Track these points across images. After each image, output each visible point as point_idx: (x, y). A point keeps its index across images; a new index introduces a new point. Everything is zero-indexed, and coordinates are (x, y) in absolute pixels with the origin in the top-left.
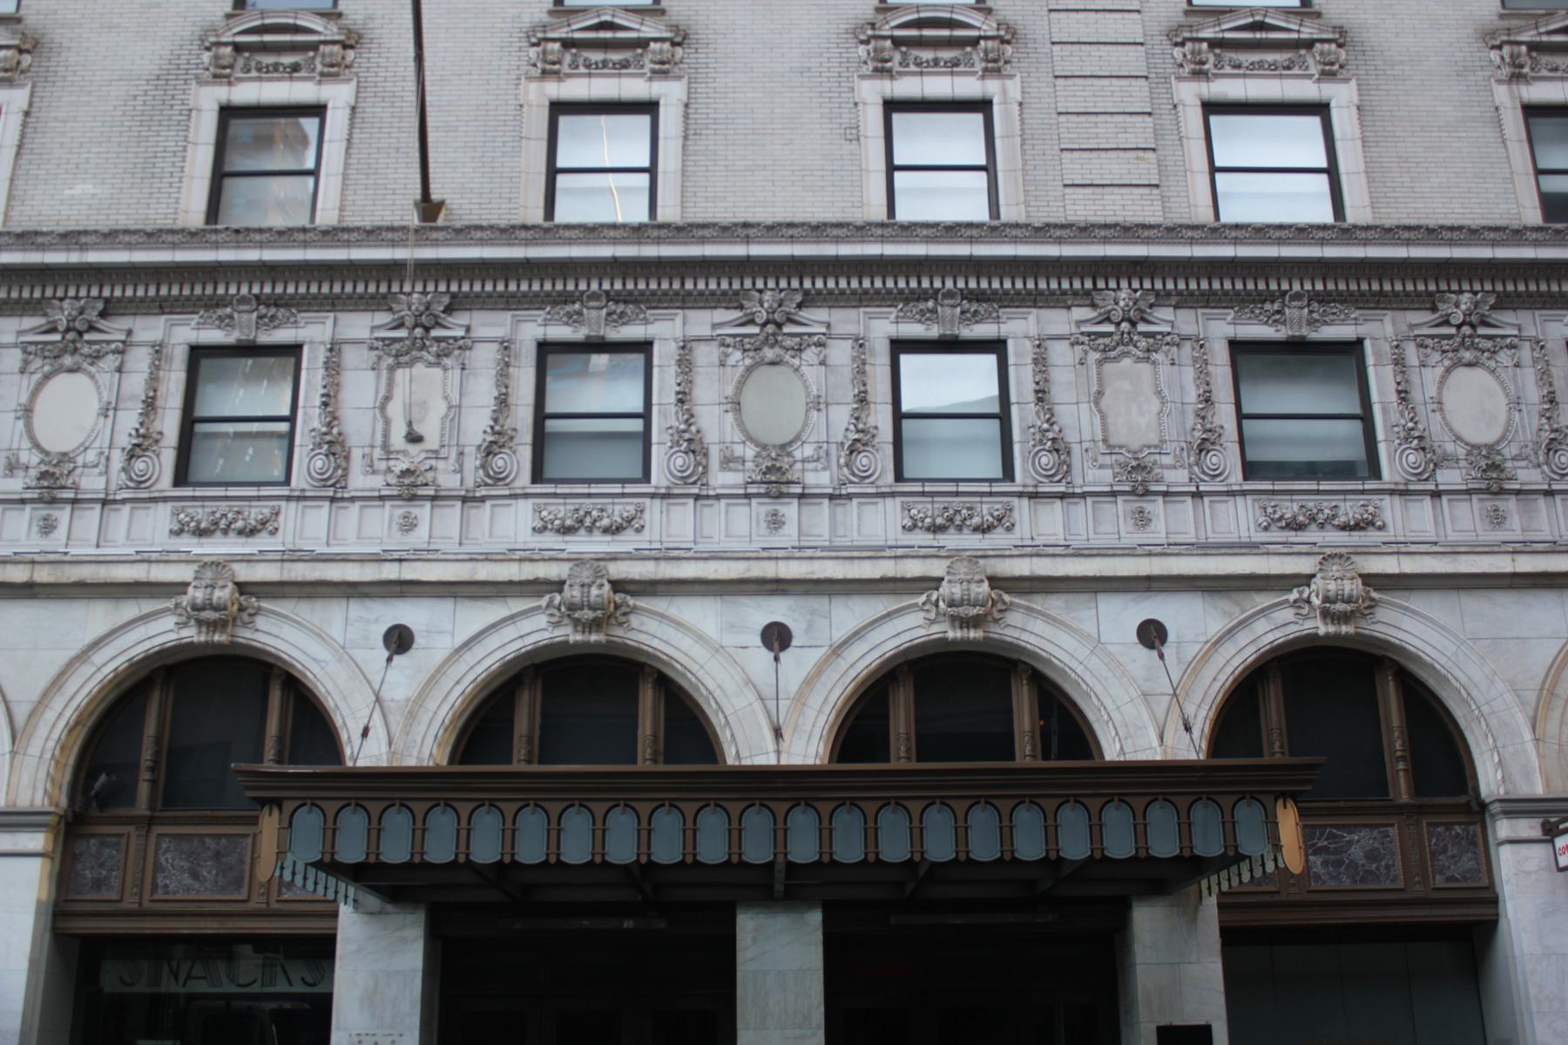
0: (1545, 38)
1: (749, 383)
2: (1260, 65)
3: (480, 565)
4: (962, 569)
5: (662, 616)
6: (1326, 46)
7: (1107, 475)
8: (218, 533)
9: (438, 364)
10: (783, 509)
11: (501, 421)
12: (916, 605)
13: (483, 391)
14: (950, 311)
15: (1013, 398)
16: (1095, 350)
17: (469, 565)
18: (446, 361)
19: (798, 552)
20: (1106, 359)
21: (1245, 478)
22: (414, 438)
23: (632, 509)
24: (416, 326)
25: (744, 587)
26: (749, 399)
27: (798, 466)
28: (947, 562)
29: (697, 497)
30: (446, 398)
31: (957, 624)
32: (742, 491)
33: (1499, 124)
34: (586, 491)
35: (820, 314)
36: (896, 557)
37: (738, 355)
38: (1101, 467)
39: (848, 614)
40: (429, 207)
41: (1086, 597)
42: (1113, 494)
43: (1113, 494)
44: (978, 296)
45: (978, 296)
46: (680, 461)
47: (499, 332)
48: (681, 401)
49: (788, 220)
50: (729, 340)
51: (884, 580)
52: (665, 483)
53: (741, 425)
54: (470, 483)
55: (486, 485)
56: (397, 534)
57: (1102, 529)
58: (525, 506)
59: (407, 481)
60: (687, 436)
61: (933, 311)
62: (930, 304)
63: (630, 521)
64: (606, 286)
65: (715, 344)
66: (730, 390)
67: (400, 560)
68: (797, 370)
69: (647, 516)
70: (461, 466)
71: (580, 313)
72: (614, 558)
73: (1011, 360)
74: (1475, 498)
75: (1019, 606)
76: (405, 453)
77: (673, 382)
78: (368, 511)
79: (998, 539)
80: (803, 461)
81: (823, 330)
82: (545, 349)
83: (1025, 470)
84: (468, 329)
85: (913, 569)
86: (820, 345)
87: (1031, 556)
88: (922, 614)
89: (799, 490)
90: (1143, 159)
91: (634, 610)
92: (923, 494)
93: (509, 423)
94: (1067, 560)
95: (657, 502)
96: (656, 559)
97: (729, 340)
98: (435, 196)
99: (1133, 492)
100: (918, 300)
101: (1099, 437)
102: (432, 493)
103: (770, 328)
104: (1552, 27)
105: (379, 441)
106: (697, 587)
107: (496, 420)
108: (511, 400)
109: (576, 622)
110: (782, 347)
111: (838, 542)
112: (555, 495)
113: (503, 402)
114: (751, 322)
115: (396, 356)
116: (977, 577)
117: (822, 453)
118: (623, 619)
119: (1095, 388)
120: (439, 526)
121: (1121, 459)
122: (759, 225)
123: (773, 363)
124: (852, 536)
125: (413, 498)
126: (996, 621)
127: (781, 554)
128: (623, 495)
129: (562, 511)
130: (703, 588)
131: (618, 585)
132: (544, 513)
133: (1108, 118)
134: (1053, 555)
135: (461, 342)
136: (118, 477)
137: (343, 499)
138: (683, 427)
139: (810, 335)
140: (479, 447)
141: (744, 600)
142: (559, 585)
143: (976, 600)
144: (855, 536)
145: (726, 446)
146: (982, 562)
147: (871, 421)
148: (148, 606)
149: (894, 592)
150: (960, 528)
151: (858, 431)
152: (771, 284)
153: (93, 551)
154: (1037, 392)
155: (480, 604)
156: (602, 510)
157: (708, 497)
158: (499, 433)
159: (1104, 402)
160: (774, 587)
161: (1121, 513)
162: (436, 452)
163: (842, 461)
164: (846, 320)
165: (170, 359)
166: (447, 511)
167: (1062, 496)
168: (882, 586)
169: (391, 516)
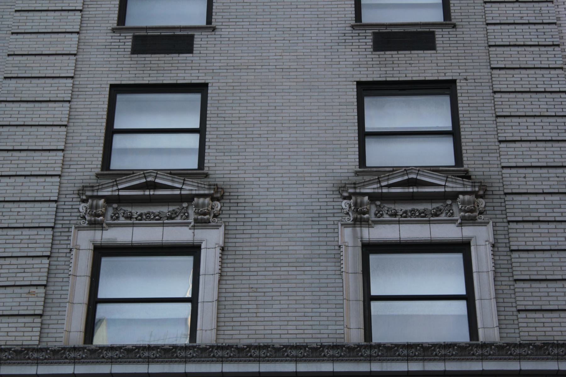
0: (385, 190)
2: (148, 216)
6: (201, 200)
33: (338, 259)
90: (34, 293)
104: (391, 182)
133: (14, 261)
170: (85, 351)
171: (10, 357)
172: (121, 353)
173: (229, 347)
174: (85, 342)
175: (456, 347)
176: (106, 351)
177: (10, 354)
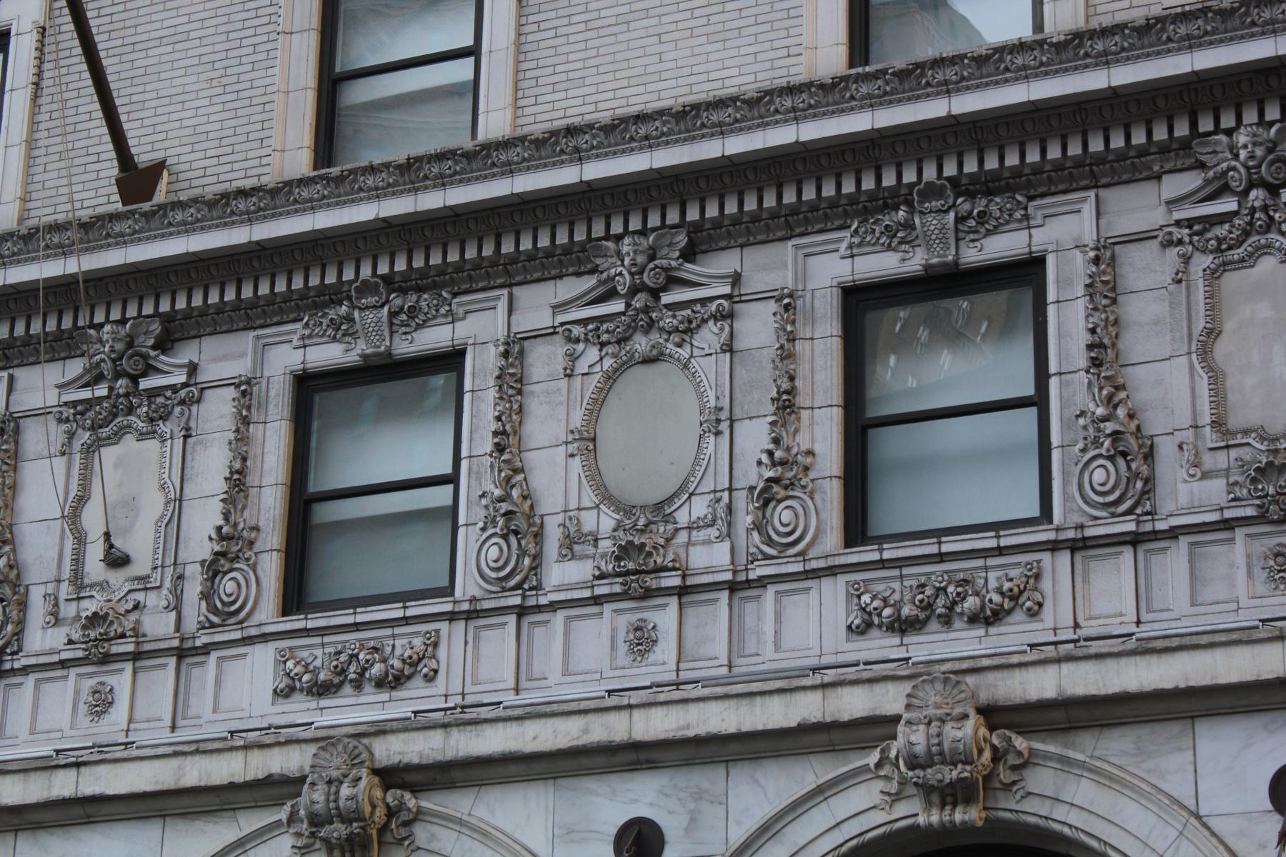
1: (612, 400)
3: (189, 761)
4: (932, 695)
5: (461, 822)
7: (1216, 490)
8: (347, 689)
9: (151, 434)
10: (653, 617)
11: (786, 440)
12: (865, 769)
13: (212, 465)
15: (1053, 368)
16: (1203, 252)
17: (174, 763)
18: (164, 428)
19: (674, 692)
20: (1225, 266)
21: (848, 544)
22: (117, 560)
23: (418, 642)
24: (118, 375)
25: (585, 761)
26: (611, 431)
27: (682, 537)
28: (907, 687)
29: (1134, 540)
30: (163, 487)
31: (935, 798)
32: (586, 594)
34: (350, 620)
35: (726, 262)
36: (824, 686)
37: (593, 354)
38: (1205, 476)
39: (756, 794)
40: (137, 180)
41: (1175, 728)
42: (1227, 525)
43: (1227, 525)
44: (985, 185)
45: (985, 185)
47: (240, 368)
48: (1096, 363)
49: (782, 82)
50: (577, 331)
51: (804, 729)
53: (595, 477)
54: (190, 624)
55: (767, 557)
56: (84, 720)
57: (1208, 594)
58: (833, 592)
59: (93, 634)
60: (1109, 427)
61: (908, 225)
62: (901, 214)
63: (414, 662)
65: (558, 339)
66: (577, 419)
67: (78, 765)
68: (686, 366)
69: (1046, 584)
70: (179, 598)
71: (349, 319)
72: (381, 730)
74: (608, 608)
75: (1047, 756)
76: (103, 585)
77: (491, 414)
78: (46, 687)
79: (1014, 635)
80: (689, 528)
81: (727, 290)
83: (1067, 498)
84: (193, 369)
85: (853, 703)
86: (720, 316)
87: (1058, 661)
88: (880, 785)
89: (676, 582)
91: (419, 815)
92: (882, 564)
94: (1124, 661)
95: (1064, 558)
96: (445, 726)
97: (577, 331)
98: (143, 154)
99: (1261, 518)
101: (1206, 418)
102: (131, 648)
103: (639, 301)
105: (66, 574)
106: (513, 769)
107: (226, 516)
108: (252, 480)
109: (927, 790)
110: (661, 329)
111: (744, 666)
112: (882, 564)
113: (238, 483)
114: (610, 295)
115: (92, 428)
116: (958, 710)
117: (721, 511)
118: (403, 832)
119: (1200, 324)
120: (144, 699)
121: (1246, 454)
122: (590, 126)
123: (648, 361)
124: (764, 656)
125: (106, 659)
126: (1008, 787)
127: (635, 698)
128: (406, 621)
129: (318, 655)
130: (522, 768)
131: (390, 776)
132: (866, 598)
134: (1099, 656)
135: (183, 393)
136: (194, 610)
137: (539, 609)
138: (1100, 411)
139: (704, 301)
140: (752, 488)
141: (590, 783)
142: (878, 728)
143: (954, 751)
144: (769, 651)
145: (571, 516)
146: (971, 680)
147: (803, 441)
148: (251, 822)
149: (832, 749)
150: (947, 621)
151: (774, 464)
152: (635, 224)
153: (166, 736)
154: (1090, 347)
155: (199, 824)
156: (375, 649)
157: (1155, 535)
158: (783, 463)
159: (1222, 349)
160: (631, 756)
161: (1240, 559)
162: (144, 579)
164: (769, 266)
165: (264, 405)
166: (157, 675)
167: (1134, 540)
168: (808, 739)
169: (77, 692)
171: (888, 88)
173: (1118, 28)
175: (1210, 15)
177: (594, 137)
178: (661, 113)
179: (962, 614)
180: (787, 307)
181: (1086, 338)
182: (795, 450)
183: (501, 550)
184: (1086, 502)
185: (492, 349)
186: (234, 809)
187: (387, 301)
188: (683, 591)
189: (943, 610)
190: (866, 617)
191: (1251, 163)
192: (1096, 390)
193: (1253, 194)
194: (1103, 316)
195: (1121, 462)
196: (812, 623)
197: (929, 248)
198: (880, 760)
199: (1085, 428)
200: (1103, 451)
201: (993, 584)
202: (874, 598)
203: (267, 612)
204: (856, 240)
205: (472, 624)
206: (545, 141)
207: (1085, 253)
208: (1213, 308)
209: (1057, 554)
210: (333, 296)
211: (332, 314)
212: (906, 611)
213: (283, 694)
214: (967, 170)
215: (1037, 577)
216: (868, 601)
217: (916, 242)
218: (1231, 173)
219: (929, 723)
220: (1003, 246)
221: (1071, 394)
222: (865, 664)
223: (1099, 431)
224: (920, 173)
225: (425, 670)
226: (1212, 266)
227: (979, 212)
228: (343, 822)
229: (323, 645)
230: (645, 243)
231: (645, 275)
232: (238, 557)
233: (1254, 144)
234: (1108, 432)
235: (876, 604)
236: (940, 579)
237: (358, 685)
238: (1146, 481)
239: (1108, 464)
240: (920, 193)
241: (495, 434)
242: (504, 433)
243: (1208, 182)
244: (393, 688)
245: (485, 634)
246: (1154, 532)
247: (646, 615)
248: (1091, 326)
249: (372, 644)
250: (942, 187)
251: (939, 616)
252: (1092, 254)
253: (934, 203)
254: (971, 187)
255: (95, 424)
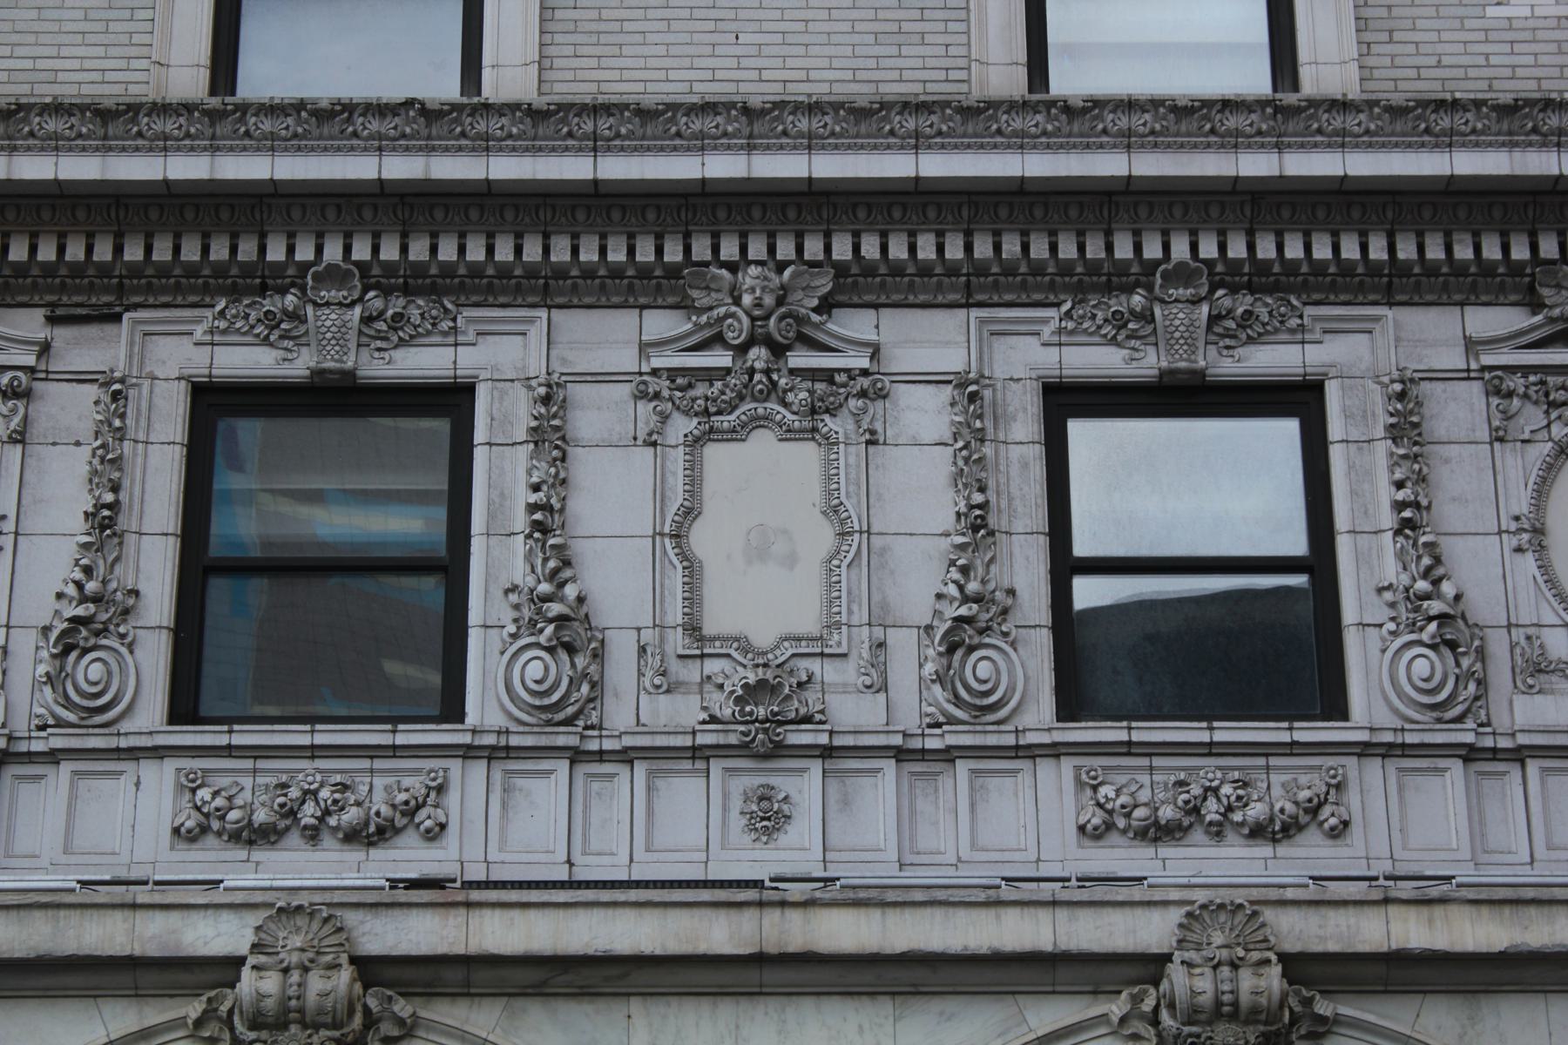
10: (784, 784)
14: (1182, 315)
46: (535, 671)
48: (541, 528)
52: (496, 720)
58: (160, 778)
63: (410, 811)
64: (361, 252)
69: (453, 798)
71: (296, 317)
73: (1336, 428)
82: (213, 402)
93: (124, 576)
95: (478, 769)
100: (1108, 289)
103: (758, 356)
112: (229, 751)
113: (105, 523)
128: (394, 751)
152: (757, 249)
156: (344, 787)
163: (930, 668)
170: (304, 114)
172: (299, 122)
174: (213, 92)
176: (687, 115)
178: (837, 106)
179: (336, 829)
180: (116, 396)
181: (525, 497)
182: (991, 586)
183: (547, 669)
184: (512, 700)
185: (520, 392)
186: (95, 997)
187: (361, 299)
188: (827, 752)
189: (313, 821)
190: (202, 818)
191: (757, 313)
192: (539, 561)
193: (754, 352)
194: (553, 470)
195: (563, 656)
196: (128, 819)
197: (1170, 347)
198: (205, 1012)
199: (517, 607)
200: (542, 639)
201: (379, 795)
202: (216, 794)
203: (149, 715)
204: (223, 324)
205: (498, 769)
206: (763, 112)
207: (530, 388)
208: (828, 478)
209: (469, 762)
210: (1114, 279)
211: (267, 304)
212: (261, 816)
213: (182, 836)
214: (612, 257)
215: (440, 789)
216: (208, 798)
217: (304, 340)
218: (730, 321)
219: (1215, 968)
220: (422, 362)
221: (498, 564)
222: (1078, 880)
223: (539, 612)
224: (319, 250)
225: (428, 823)
226: (696, 432)
227: (395, 314)
228: (305, 1026)
229: (255, 771)
230: (776, 281)
231: (772, 320)
232: (106, 630)
233: (763, 289)
234: (550, 615)
235: (220, 802)
236: (310, 779)
237: (312, 835)
238: (593, 685)
239: (542, 654)
240: (316, 277)
241: (532, 508)
242: (546, 507)
243: (699, 327)
244: (371, 844)
245: (993, 782)
246: (923, 751)
247: (774, 780)
248: (535, 479)
249: (338, 778)
250: (1198, 272)
251: (305, 827)
252: (542, 391)
253: (1181, 291)
254: (1228, 278)
255: (704, 406)
